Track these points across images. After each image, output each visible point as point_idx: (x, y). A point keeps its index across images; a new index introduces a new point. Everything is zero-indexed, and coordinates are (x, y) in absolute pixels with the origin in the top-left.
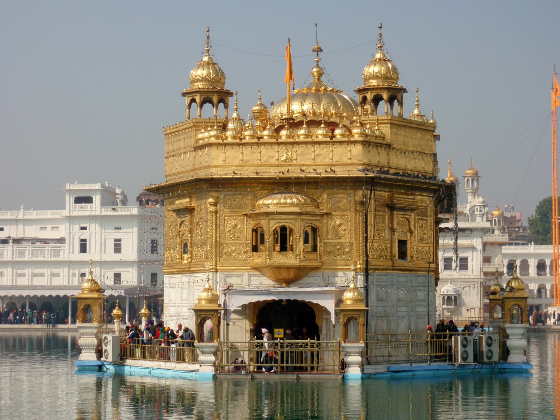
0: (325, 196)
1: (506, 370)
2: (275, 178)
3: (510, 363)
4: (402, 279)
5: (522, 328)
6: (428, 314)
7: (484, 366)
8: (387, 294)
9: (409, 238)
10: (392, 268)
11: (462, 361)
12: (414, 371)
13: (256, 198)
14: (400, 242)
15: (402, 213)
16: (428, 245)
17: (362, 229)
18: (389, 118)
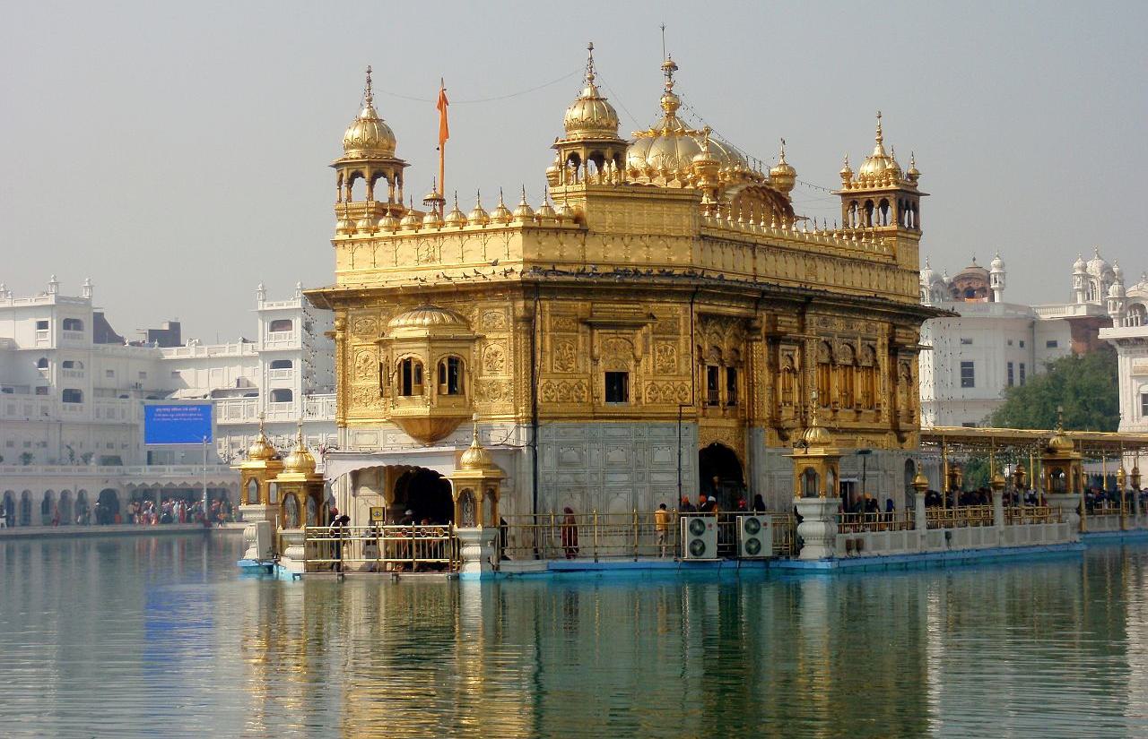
0: (477, 311)
1: (795, 571)
2: (416, 288)
3: (801, 561)
4: (616, 432)
5: (818, 504)
6: (680, 485)
7: (744, 564)
8: (581, 455)
9: (632, 368)
10: (592, 415)
11: (692, 556)
12: (602, 570)
13: (391, 317)
14: (609, 376)
15: (614, 331)
16: (679, 378)
17: (524, 360)
18: (584, 189)
